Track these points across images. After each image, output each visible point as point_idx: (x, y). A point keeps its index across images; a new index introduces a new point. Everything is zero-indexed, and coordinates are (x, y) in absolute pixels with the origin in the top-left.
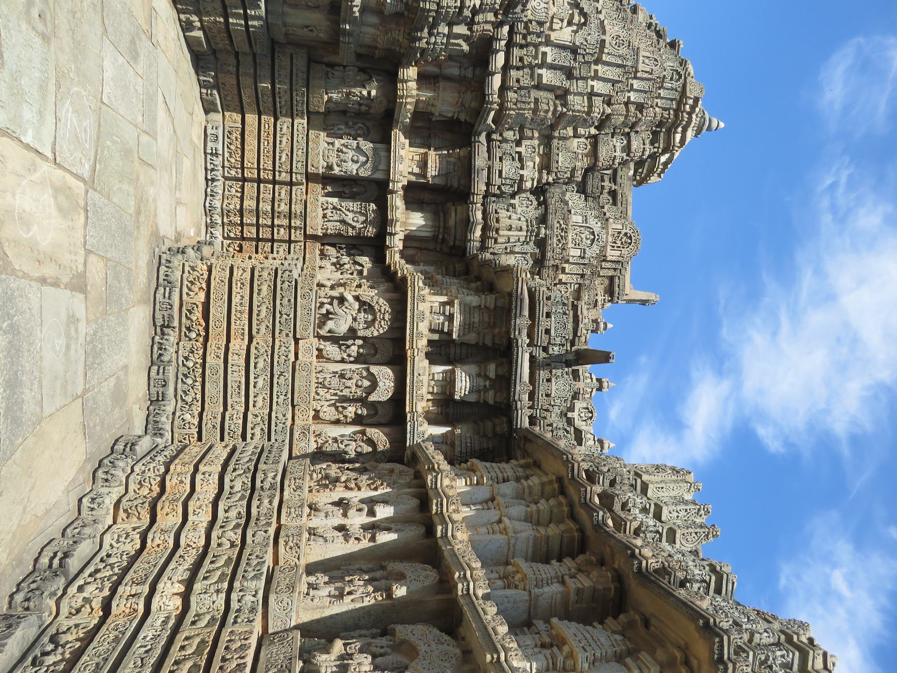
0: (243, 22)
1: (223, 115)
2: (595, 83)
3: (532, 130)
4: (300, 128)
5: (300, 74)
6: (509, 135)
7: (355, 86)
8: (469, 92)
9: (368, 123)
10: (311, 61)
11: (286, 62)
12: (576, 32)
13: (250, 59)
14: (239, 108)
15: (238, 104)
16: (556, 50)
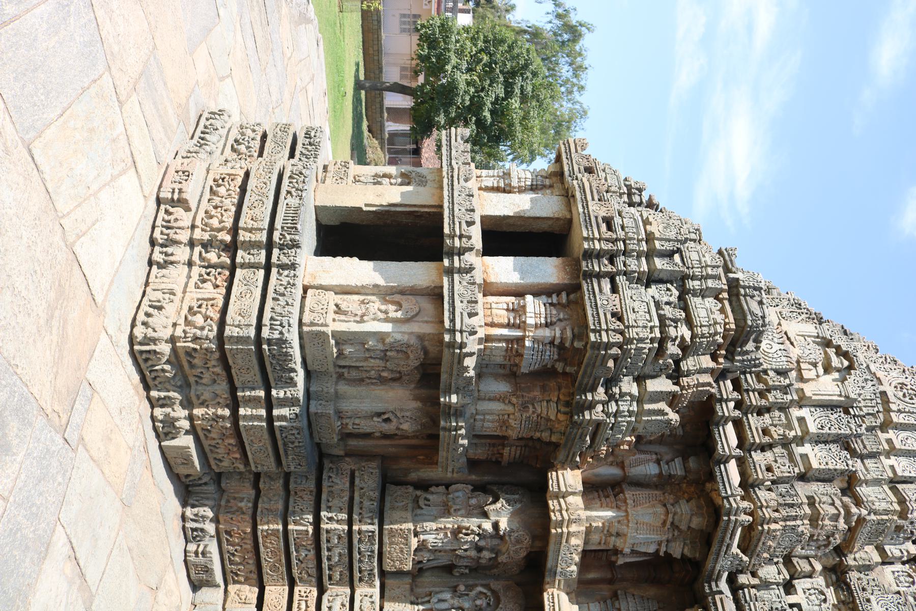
0: (263, 412)
1: (226, 591)
2: (893, 461)
3: (807, 558)
4: (366, 604)
5: (367, 503)
6: (769, 572)
7: (469, 515)
8: (683, 502)
9: (495, 585)
10: (388, 481)
11: (342, 483)
12: (843, 380)
13: (279, 484)
14: (255, 576)
15: (253, 568)
16: (819, 412)
